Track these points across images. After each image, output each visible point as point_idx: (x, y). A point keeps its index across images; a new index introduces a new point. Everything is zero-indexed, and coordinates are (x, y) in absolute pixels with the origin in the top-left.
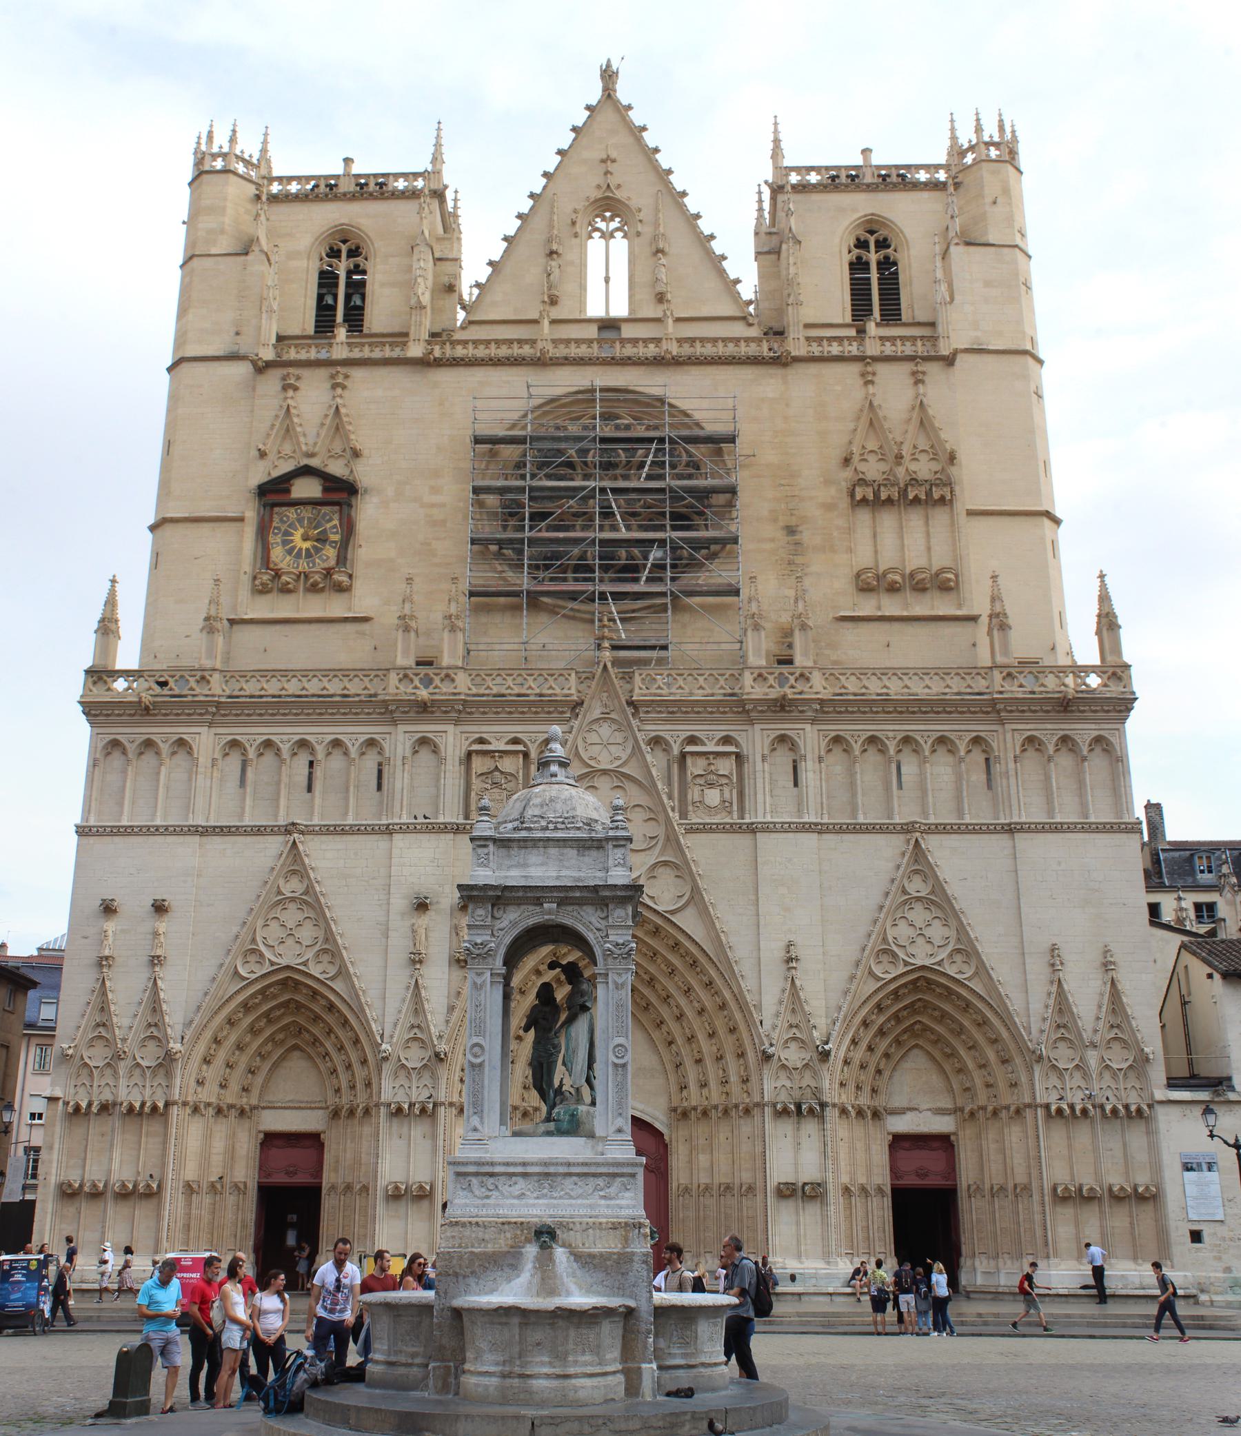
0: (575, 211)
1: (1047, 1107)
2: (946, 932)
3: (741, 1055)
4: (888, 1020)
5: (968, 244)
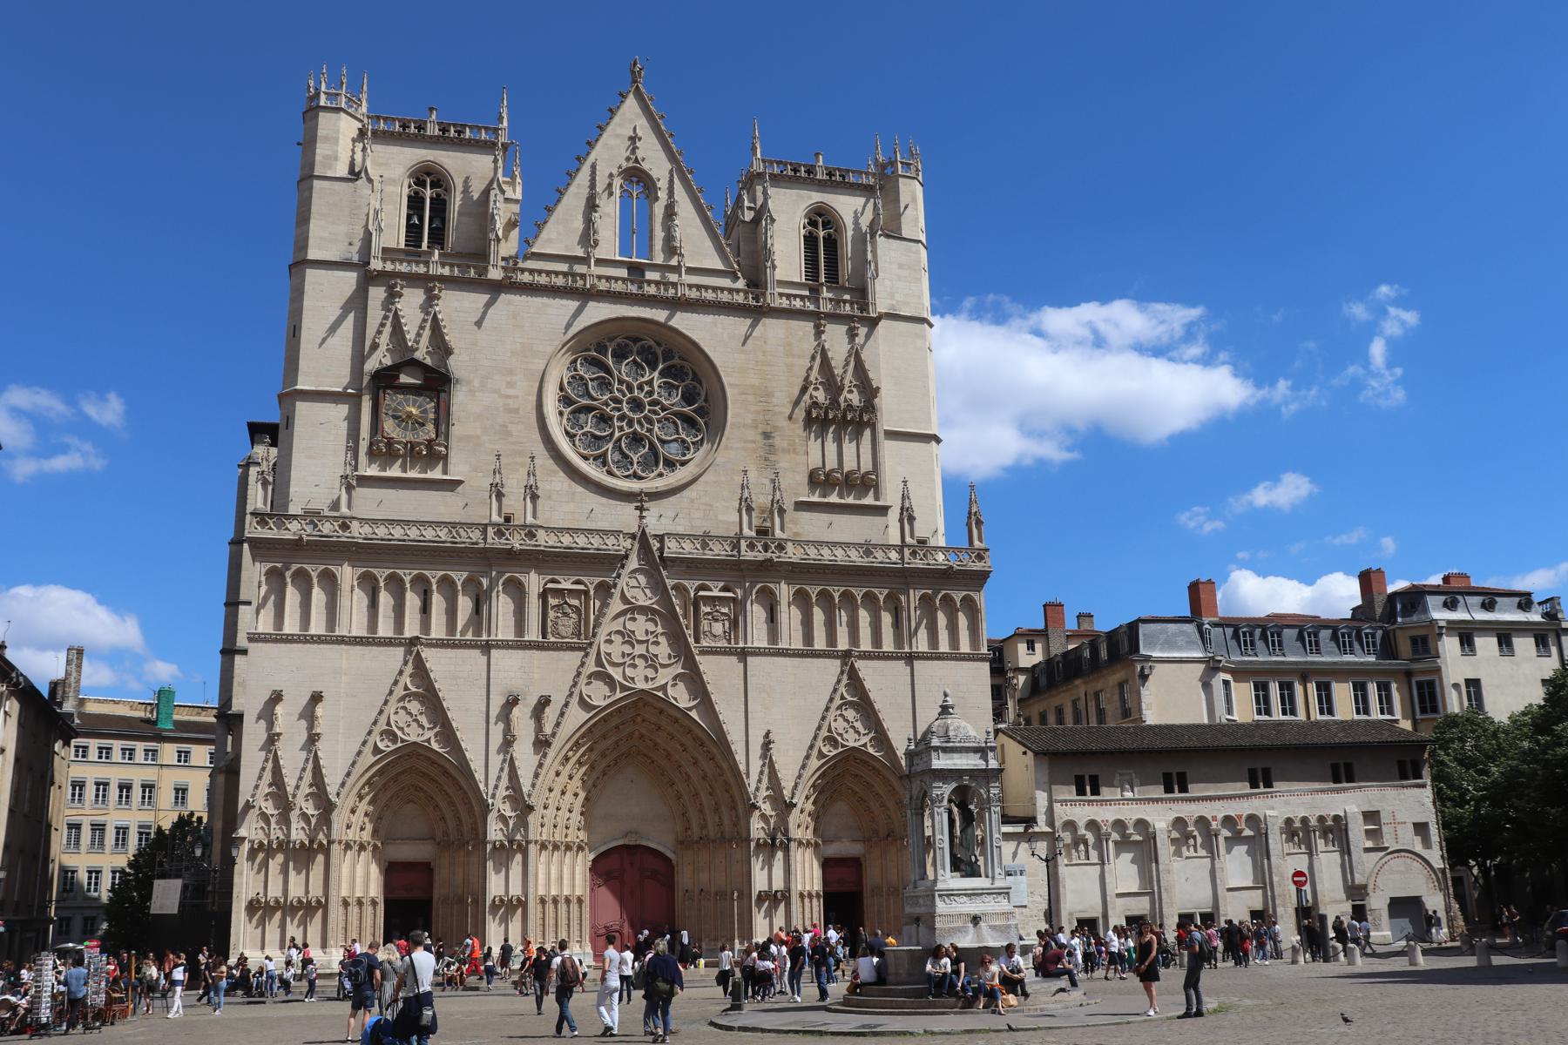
0: (611, 175)
3: (734, 808)
5: (888, 236)
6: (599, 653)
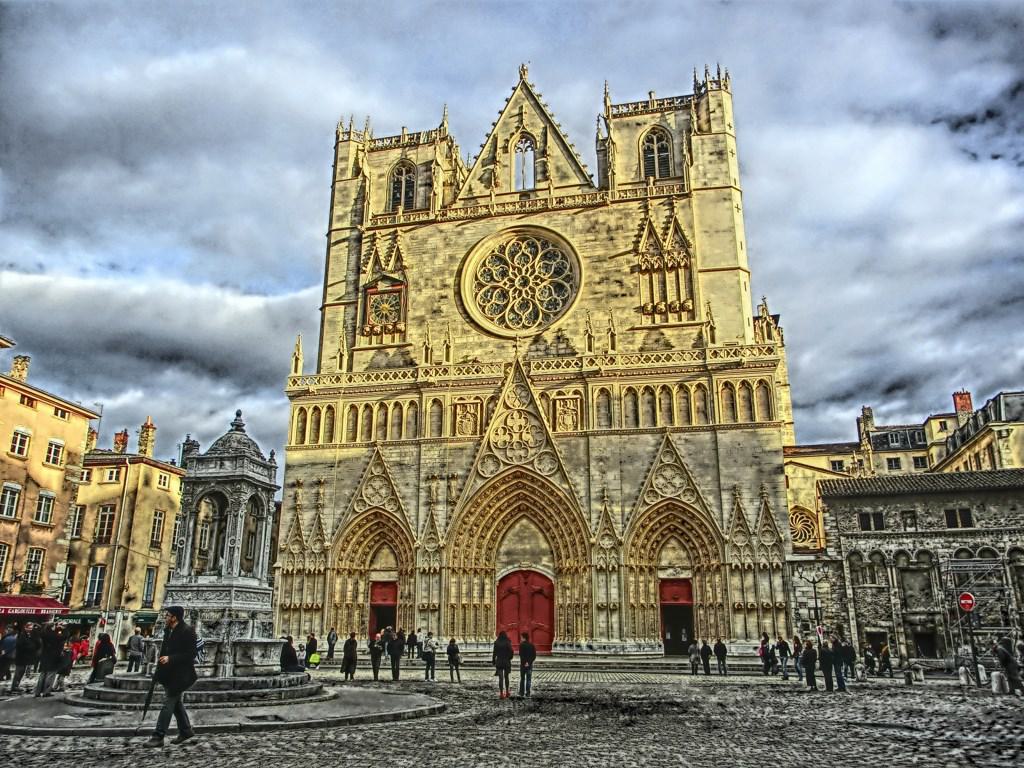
1: (731, 565)
2: (682, 481)
4: (656, 524)
6: (489, 442)
